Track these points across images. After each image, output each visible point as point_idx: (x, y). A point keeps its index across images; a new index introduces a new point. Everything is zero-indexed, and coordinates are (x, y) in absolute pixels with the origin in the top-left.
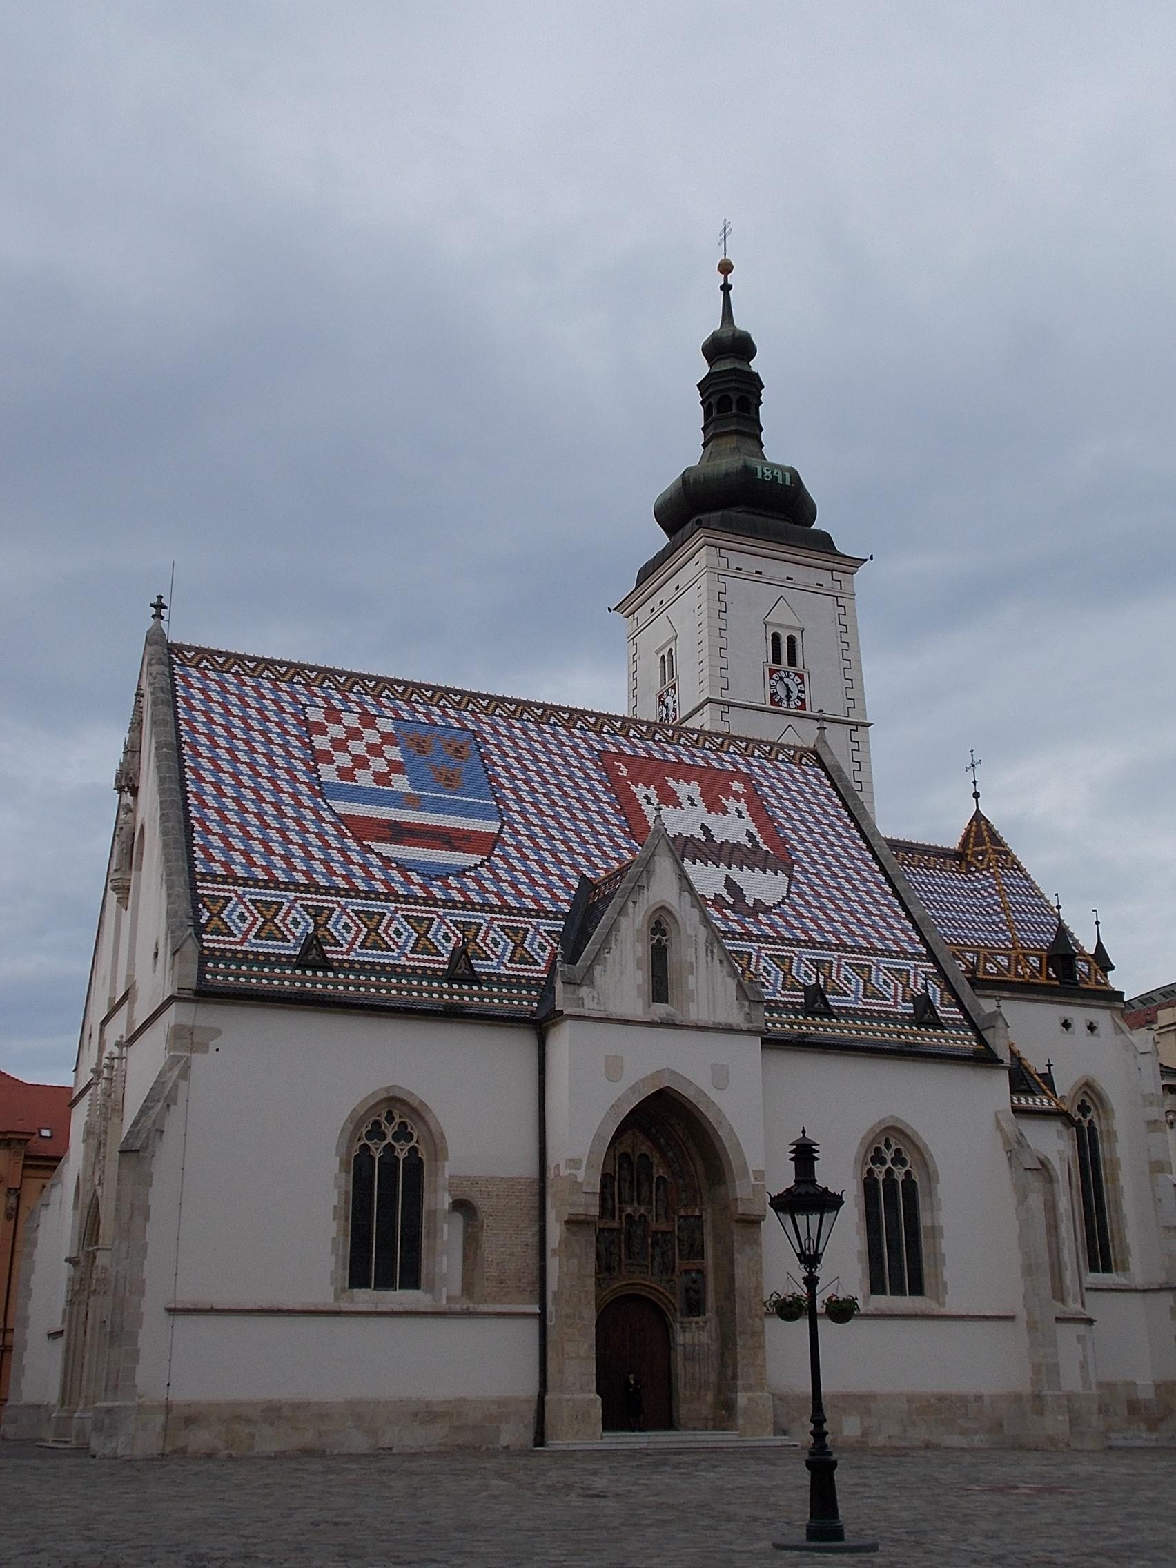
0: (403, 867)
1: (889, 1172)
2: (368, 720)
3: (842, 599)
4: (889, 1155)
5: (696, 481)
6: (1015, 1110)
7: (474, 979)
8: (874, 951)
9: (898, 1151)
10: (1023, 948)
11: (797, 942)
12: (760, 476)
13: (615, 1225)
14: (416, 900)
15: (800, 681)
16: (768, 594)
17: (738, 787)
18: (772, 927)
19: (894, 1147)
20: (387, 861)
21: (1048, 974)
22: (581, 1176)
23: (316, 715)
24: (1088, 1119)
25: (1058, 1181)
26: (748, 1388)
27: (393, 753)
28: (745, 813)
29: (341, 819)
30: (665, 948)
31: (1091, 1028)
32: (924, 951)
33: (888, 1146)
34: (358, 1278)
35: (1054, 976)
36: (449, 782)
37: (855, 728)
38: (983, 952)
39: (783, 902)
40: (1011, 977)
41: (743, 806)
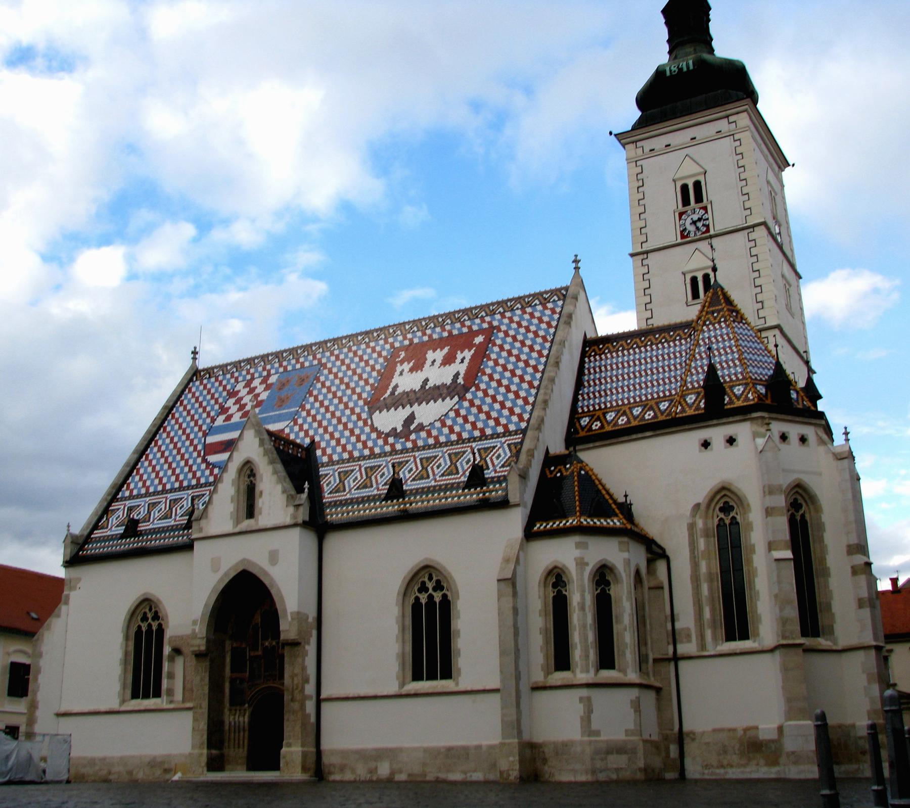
1: (431, 597)
4: (430, 585)
5: (641, 99)
9: (438, 582)
10: (687, 388)
12: (668, 74)
13: (260, 653)
14: (207, 484)
15: (704, 212)
17: (479, 339)
18: (414, 442)
19: (435, 579)
20: (208, 464)
21: (698, 408)
22: (197, 631)
23: (240, 386)
24: (730, 517)
25: (574, 582)
26: (289, 745)
27: (264, 396)
29: (205, 446)
30: (254, 484)
31: (731, 441)
33: (430, 578)
34: (135, 696)
35: (702, 405)
37: (752, 230)
38: (653, 403)
39: (438, 420)
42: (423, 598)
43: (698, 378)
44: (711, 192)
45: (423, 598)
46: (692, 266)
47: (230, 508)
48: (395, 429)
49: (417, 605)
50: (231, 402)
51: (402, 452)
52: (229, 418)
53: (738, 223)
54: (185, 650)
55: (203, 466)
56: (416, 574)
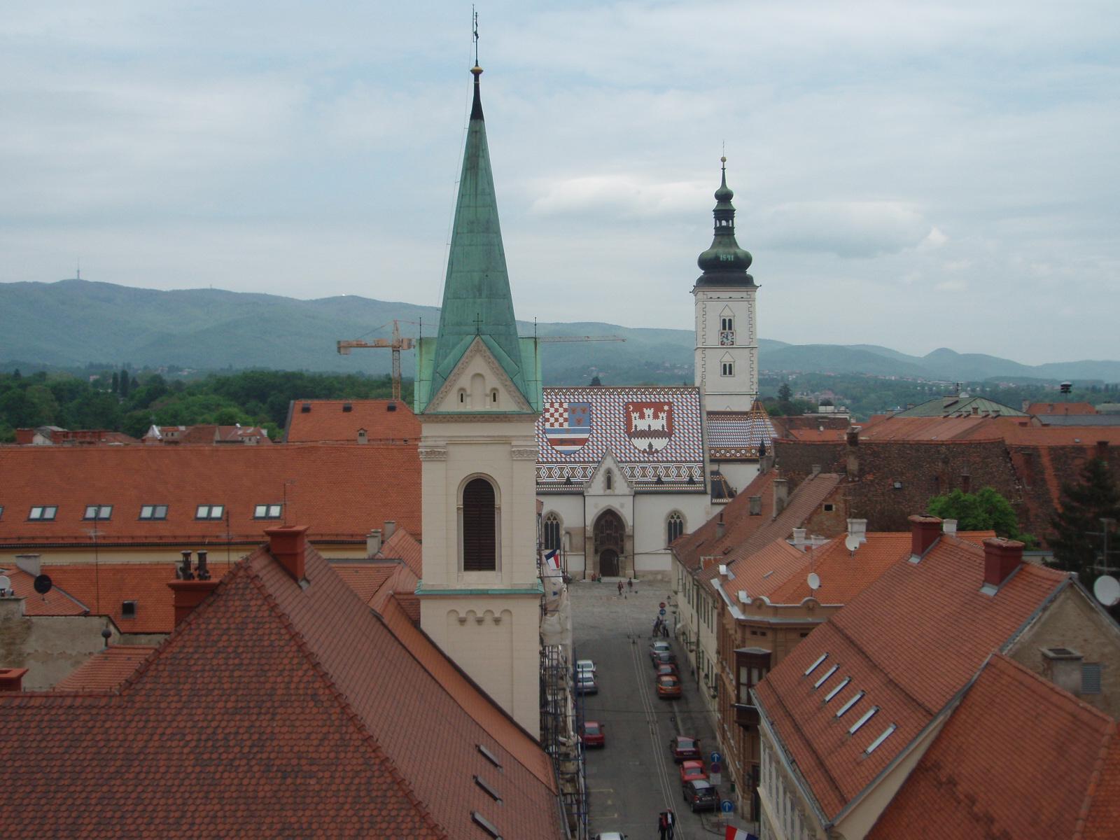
0: (561, 453)
2: (561, 405)
3: (751, 301)
6: (712, 504)
7: (571, 483)
8: (686, 461)
11: (663, 462)
14: (561, 462)
16: (721, 305)
17: (666, 408)
23: (548, 406)
28: (665, 418)
29: (549, 440)
32: (702, 459)
36: (579, 422)
40: (744, 457)
41: (665, 415)
42: (673, 521)
43: (757, 443)
44: (735, 325)
45: (673, 521)
46: (724, 359)
47: (602, 485)
48: (645, 449)
49: (670, 523)
50: (547, 415)
51: (654, 462)
52: (552, 425)
53: (746, 344)
54: (572, 533)
55: (554, 451)
56: (671, 513)
